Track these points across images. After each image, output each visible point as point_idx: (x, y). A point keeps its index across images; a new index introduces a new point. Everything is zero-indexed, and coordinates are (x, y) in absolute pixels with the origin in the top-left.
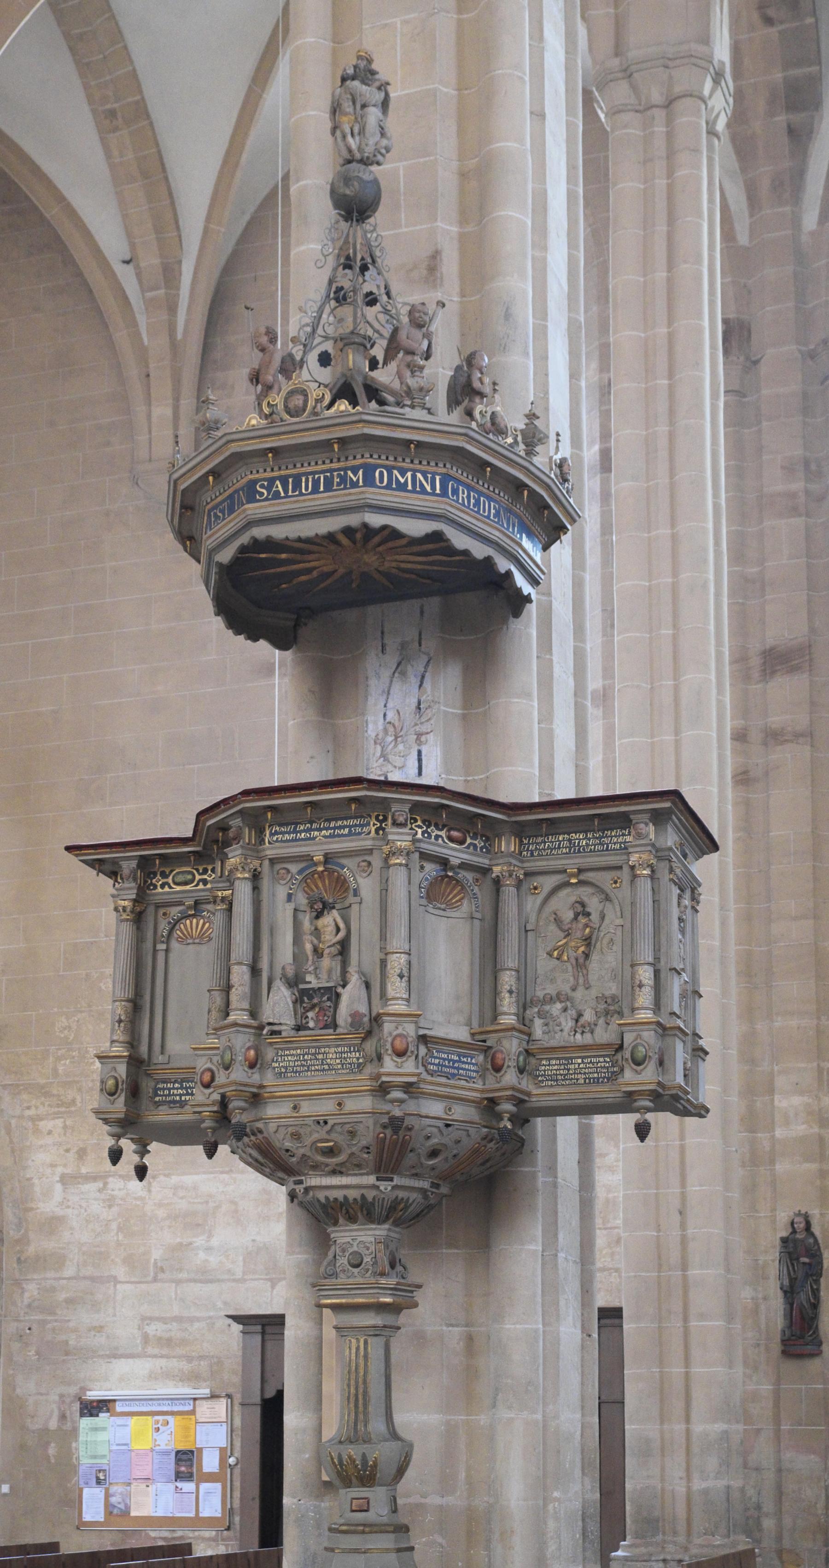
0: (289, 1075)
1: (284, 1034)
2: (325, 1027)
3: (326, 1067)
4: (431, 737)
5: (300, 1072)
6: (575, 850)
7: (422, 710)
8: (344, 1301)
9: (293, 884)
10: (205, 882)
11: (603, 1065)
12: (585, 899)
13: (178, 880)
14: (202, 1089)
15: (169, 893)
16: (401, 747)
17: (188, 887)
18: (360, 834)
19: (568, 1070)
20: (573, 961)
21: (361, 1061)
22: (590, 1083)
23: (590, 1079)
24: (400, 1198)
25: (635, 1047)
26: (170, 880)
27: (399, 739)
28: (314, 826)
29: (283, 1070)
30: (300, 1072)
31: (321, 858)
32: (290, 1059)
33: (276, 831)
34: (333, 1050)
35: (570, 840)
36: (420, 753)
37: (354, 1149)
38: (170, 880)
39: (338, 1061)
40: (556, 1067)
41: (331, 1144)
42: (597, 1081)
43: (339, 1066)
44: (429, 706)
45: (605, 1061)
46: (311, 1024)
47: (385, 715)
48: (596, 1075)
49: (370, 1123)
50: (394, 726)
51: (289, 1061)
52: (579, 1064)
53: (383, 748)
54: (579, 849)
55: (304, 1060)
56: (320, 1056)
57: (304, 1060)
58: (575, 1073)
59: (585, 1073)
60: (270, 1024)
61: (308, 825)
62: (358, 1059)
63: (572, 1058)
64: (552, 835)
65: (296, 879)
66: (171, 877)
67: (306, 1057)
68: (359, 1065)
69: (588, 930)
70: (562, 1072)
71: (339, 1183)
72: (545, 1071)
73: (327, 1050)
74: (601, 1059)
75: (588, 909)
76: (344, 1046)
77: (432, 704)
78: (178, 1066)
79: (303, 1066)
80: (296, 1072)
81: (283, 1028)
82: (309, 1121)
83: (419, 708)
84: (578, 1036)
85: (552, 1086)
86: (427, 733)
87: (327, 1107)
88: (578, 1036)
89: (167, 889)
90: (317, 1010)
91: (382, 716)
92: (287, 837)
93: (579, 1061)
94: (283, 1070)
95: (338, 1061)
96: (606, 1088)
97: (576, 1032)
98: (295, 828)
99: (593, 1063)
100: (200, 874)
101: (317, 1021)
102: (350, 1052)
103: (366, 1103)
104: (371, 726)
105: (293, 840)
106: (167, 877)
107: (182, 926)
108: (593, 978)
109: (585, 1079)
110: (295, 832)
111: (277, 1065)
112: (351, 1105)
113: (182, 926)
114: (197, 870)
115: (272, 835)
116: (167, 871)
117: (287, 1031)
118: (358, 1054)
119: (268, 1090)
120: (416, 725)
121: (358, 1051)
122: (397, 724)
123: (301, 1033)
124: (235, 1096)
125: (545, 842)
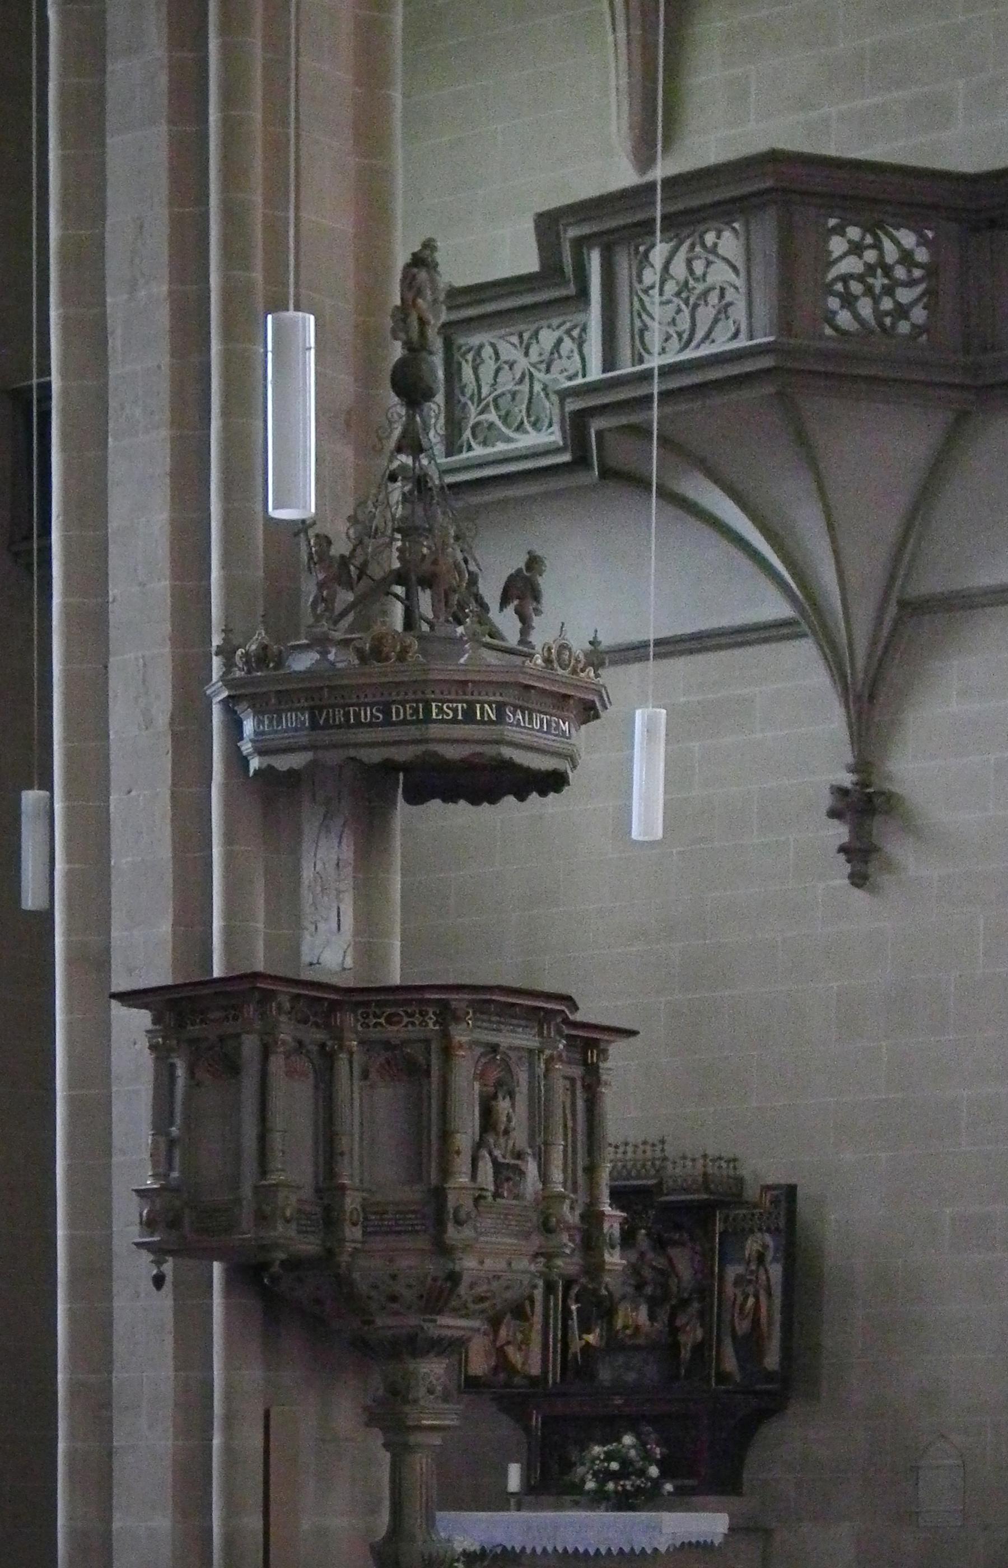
49: (526, 1283)
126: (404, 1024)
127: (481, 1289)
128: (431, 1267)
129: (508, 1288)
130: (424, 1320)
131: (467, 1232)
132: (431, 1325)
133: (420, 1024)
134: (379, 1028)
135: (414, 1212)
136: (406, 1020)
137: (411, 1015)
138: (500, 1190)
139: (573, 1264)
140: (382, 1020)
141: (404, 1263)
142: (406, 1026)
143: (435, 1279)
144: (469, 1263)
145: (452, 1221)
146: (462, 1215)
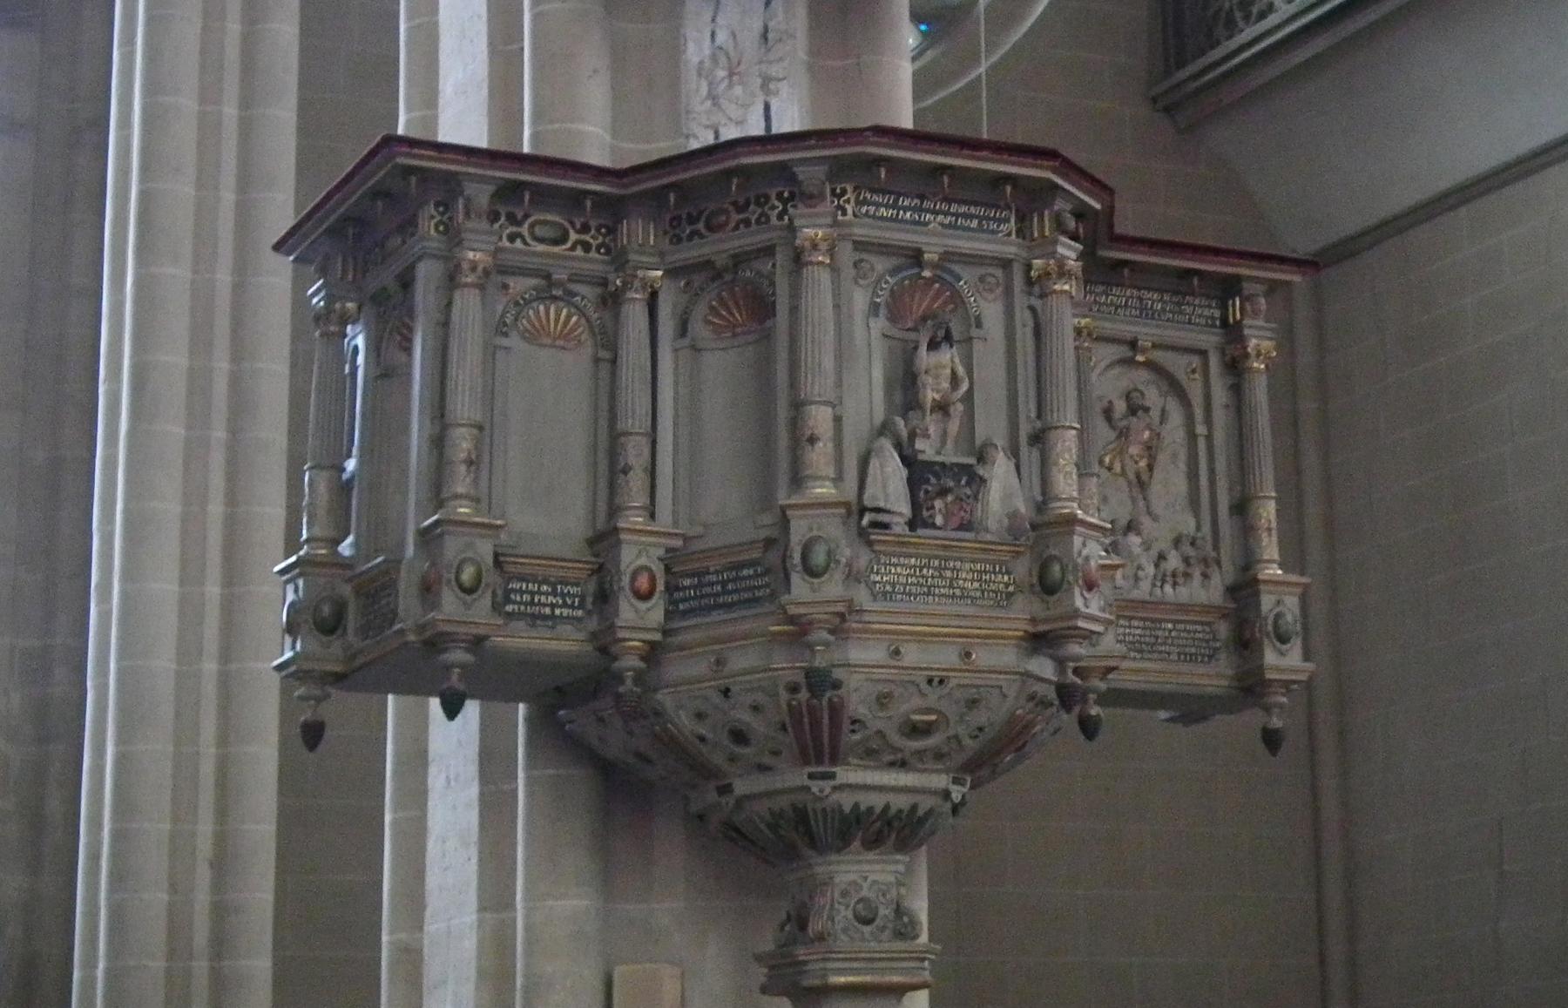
0: (899, 596)
1: (897, 529)
2: (961, 527)
3: (958, 592)
4: (784, 88)
5: (916, 596)
6: (1146, 313)
7: (770, 43)
8: (868, 979)
9: (882, 289)
10: (587, 247)
11: (1201, 635)
12: (1141, 387)
13: (538, 231)
14: (634, 601)
15: (520, 252)
16: (738, 90)
17: (556, 249)
18: (993, 232)
19: (1157, 637)
20: (1132, 476)
21: (1011, 589)
22: (1185, 661)
23: (1186, 654)
24: (893, 810)
25: (1278, 616)
26: (525, 230)
27: (735, 78)
28: (926, 204)
29: (888, 588)
30: (916, 596)
31: (936, 257)
32: (896, 572)
33: (865, 198)
34: (967, 566)
35: (1141, 299)
36: (767, 108)
37: (961, 730)
38: (525, 230)
39: (976, 585)
40: (1138, 632)
41: (933, 717)
42: (1192, 658)
43: (978, 594)
44: (780, 40)
45: (1204, 631)
46: (939, 520)
47: (713, 35)
48: (1193, 650)
50: (727, 55)
51: (899, 575)
52: (1170, 631)
53: (710, 84)
54: (1153, 314)
55: (923, 577)
56: (948, 574)
57: (923, 577)
58: (1164, 644)
59: (1179, 646)
60: (878, 510)
61: (916, 201)
62: (1007, 586)
63: (1160, 621)
64: (1117, 286)
65: (887, 282)
66: (526, 225)
67: (925, 571)
68: (1010, 595)
69: (1147, 434)
70: (1147, 639)
71: (893, 783)
72: (1124, 635)
73: (958, 564)
74: (1199, 628)
75: (1148, 404)
76: (981, 561)
77: (785, 38)
78: (529, 552)
79: (922, 585)
80: (910, 594)
81: (896, 519)
82: (920, 678)
83: (765, 36)
84: (1168, 588)
85: (1135, 659)
86: (780, 80)
87: (946, 657)
88: (1168, 588)
89: (518, 244)
90: (950, 498)
91: (709, 34)
92: (883, 211)
93: (1170, 626)
94: (888, 588)
95: (976, 585)
96: (1202, 670)
97: (1164, 581)
98: (896, 201)
99: (1189, 632)
100: (578, 232)
101: (946, 517)
102: (995, 573)
103: (1007, 657)
104: (691, 47)
105: (891, 219)
106: (519, 224)
107: (531, 312)
108: (1158, 506)
109: (1179, 654)
110: (895, 206)
111: (878, 578)
112: (981, 657)
113: (531, 312)
114: (572, 224)
115: (859, 203)
116: (520, 216)
117: (899, 526)
118: (1006, 578)
119: (867, 618)
120: (761, 62)
121: (1008, 573)
122: (732, 54)
123: (920, 532)
124: (826, 621)
125: (1107, 296)
126: (732, 225)
127: (909, 706)
128: (786, 665)
129: (973, 703)
130: (811, 776)
131: (833, 588)
132: (827, 785)
133: (758, 222)
134: (696, 240)
135: (752, 563)
136: (735, 217)
137: (741, 209)
138: (925, 514)
139: (1218, 675)
140: (701, 226)
141: (742, 660)
142: (736, 228)
143: (794, 689)
144: (865, 653)
145: (799, 568)
146: (819, 557)
